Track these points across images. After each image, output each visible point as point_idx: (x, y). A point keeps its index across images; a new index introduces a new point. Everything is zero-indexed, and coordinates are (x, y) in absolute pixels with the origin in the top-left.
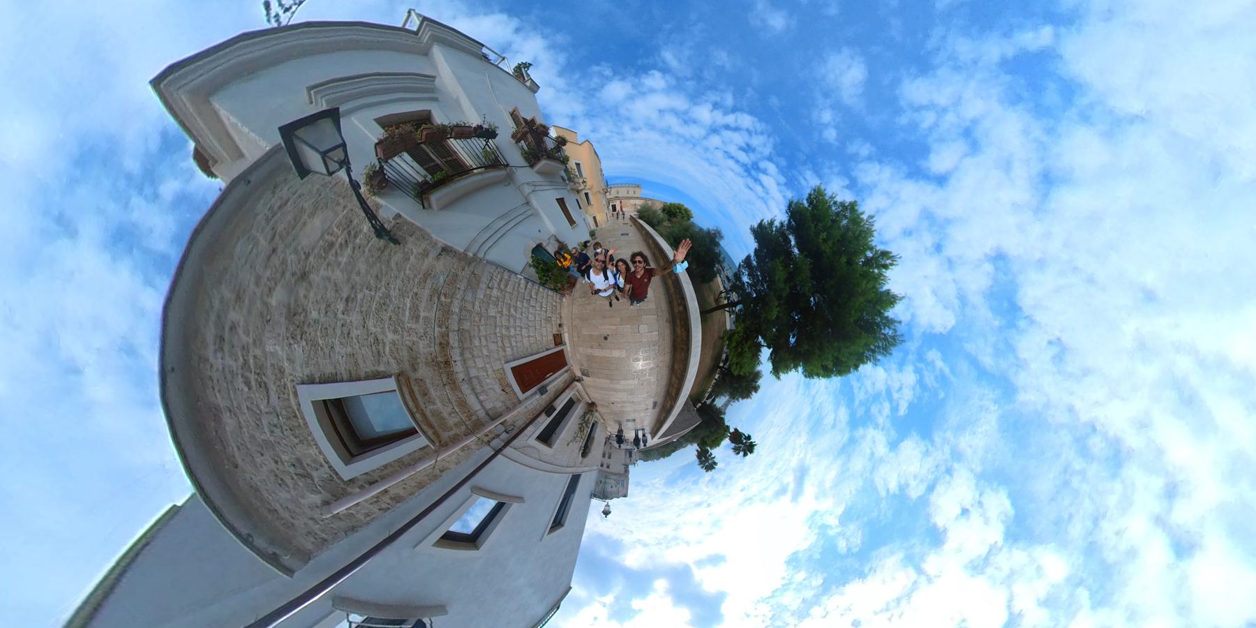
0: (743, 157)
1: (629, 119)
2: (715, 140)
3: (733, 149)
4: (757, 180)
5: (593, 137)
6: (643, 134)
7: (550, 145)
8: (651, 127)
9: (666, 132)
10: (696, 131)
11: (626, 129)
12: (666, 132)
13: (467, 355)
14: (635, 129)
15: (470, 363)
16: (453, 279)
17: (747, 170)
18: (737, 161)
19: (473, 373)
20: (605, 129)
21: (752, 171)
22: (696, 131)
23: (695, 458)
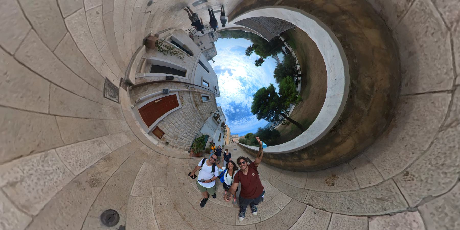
0: (247, 120)
1: (234, 125)
2: (244, 122)
3: (246, 121)
4: (251, 119)
5: (230, 127)
6: (236, 126)
7: (224, 126)
8: (237, 125)
9: (239, 125)
10: (242, 123)
11: (234, 126)
12: (239, 125)
13: (193, 108)
14: (235, 126)
15: (192, 106)
16: (203, 117)
17: (249, 120)
18: (247, 121)
19: (191, 104)
20: (231, 126)
21: (249, 119)
22: (242, 123)
23: (247, 48)
